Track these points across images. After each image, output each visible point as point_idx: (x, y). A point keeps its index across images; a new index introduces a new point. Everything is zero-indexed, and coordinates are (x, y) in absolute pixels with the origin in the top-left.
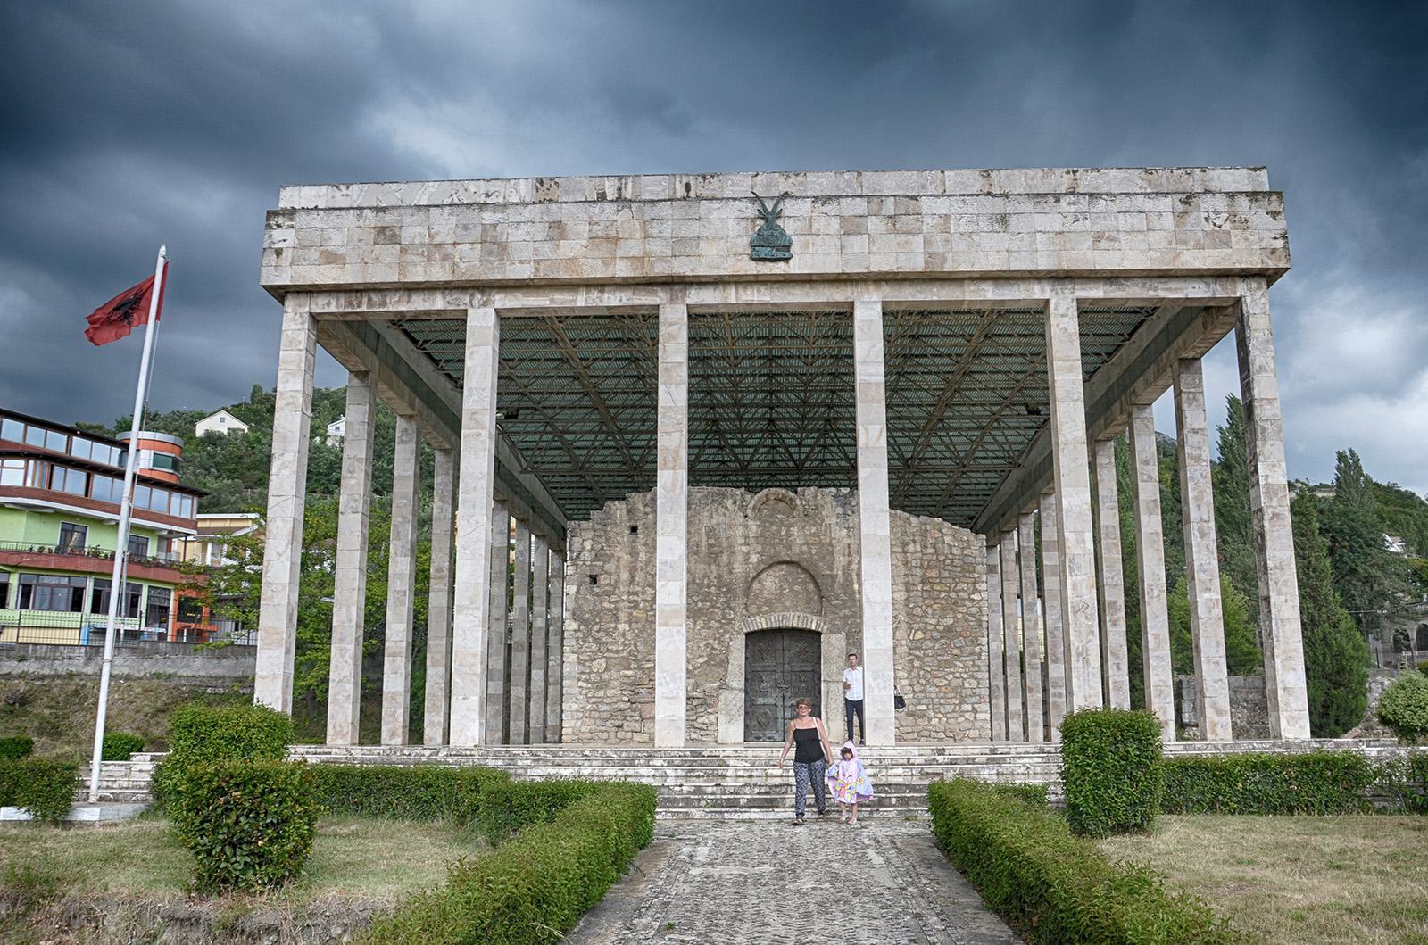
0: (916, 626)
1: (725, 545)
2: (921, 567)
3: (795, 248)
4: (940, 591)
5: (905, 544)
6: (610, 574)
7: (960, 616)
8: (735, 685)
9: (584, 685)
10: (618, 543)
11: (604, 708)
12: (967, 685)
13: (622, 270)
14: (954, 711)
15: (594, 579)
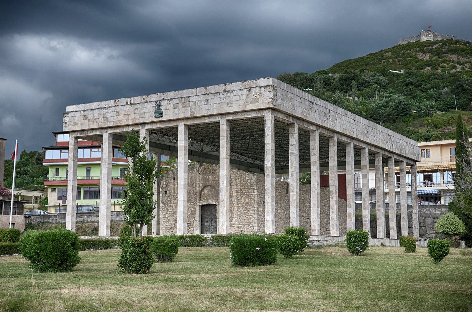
0: (239, 203)
1: (194, 182)
2: (240, 186)
3: (164, 114)
4: (245, 192)
5: (236, 179)
6: (169, 191)
8: (197, 220)
11: (169, 227)
13: (130, 122)
14: (248, 226)
15: (166, 192)
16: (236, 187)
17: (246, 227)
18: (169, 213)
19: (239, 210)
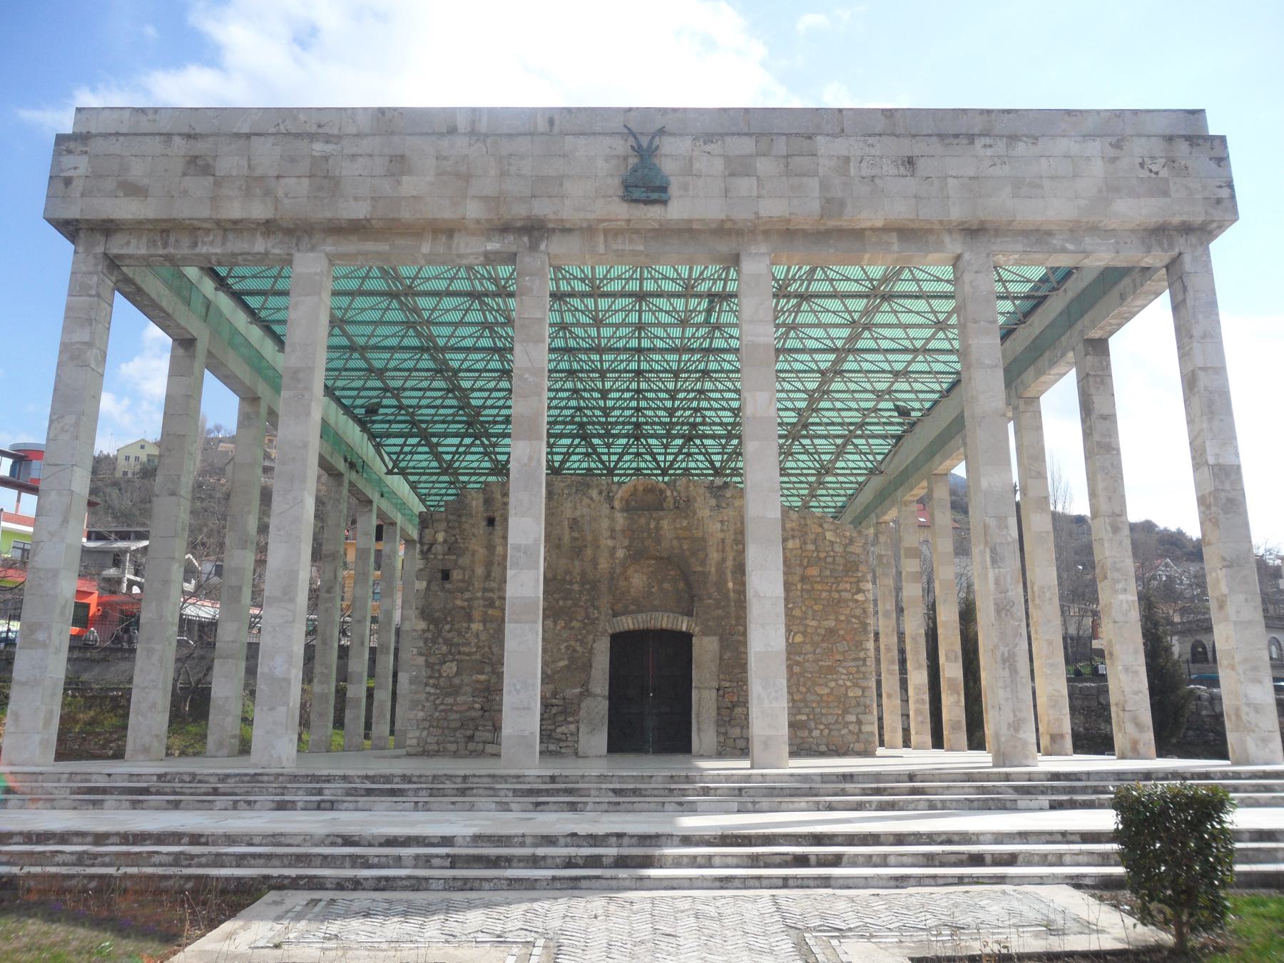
0: (795, 628)
1: (589, 538)
2: (801, 565)
3: (674, 190)
4: (822, 591)
6: (463, 569)
7: (842, 618)
9: (432, 691)
10: (474, 535)
11: (453, 716)
12: (851, 694)
14: (836, 722)
15: (446, 575)
17: (827, 726)
18: (459, 661)
19: (797, 658)
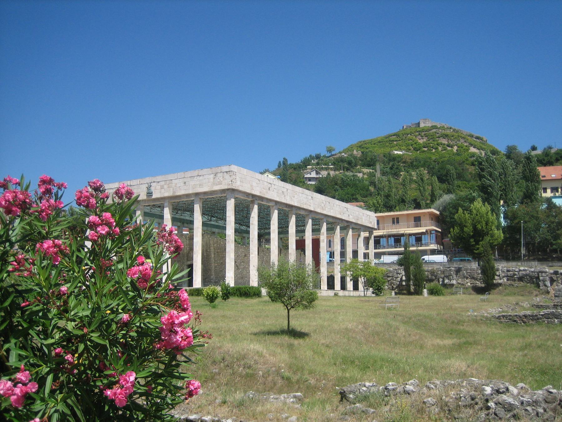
5: (214, 244)
16: (213, 250)
